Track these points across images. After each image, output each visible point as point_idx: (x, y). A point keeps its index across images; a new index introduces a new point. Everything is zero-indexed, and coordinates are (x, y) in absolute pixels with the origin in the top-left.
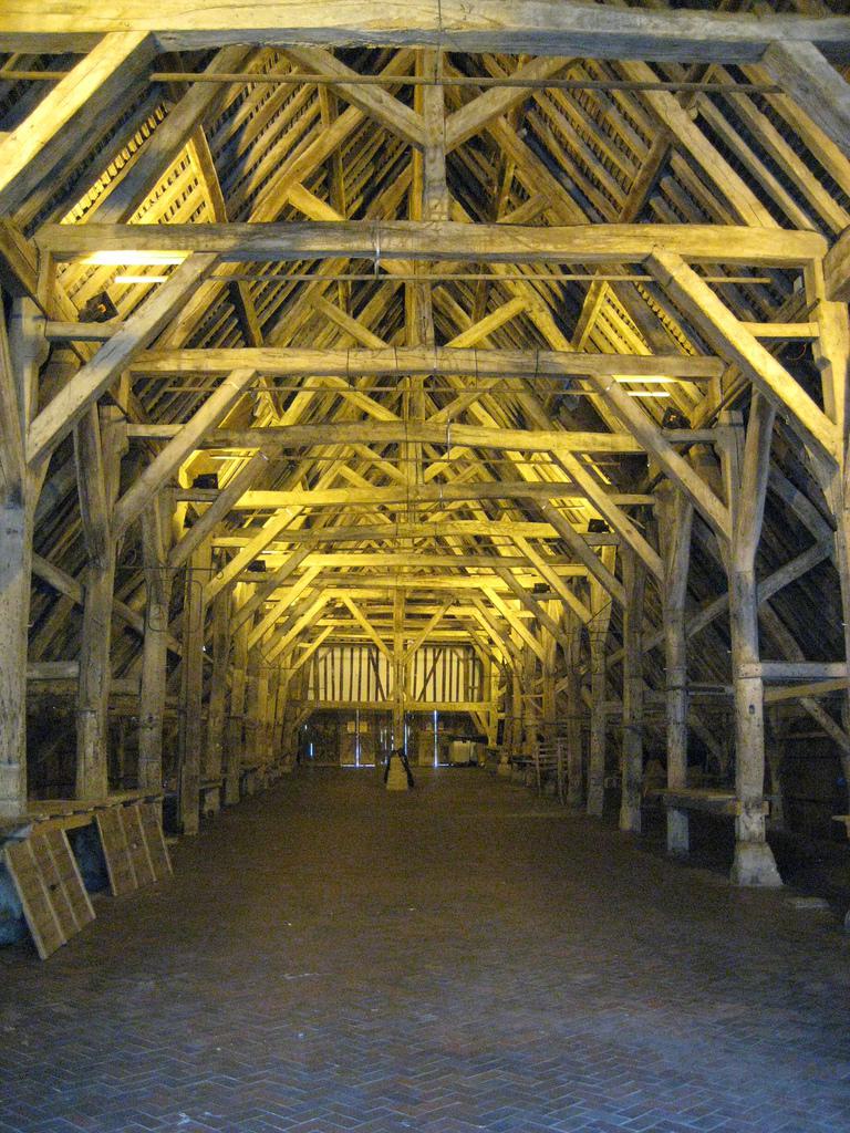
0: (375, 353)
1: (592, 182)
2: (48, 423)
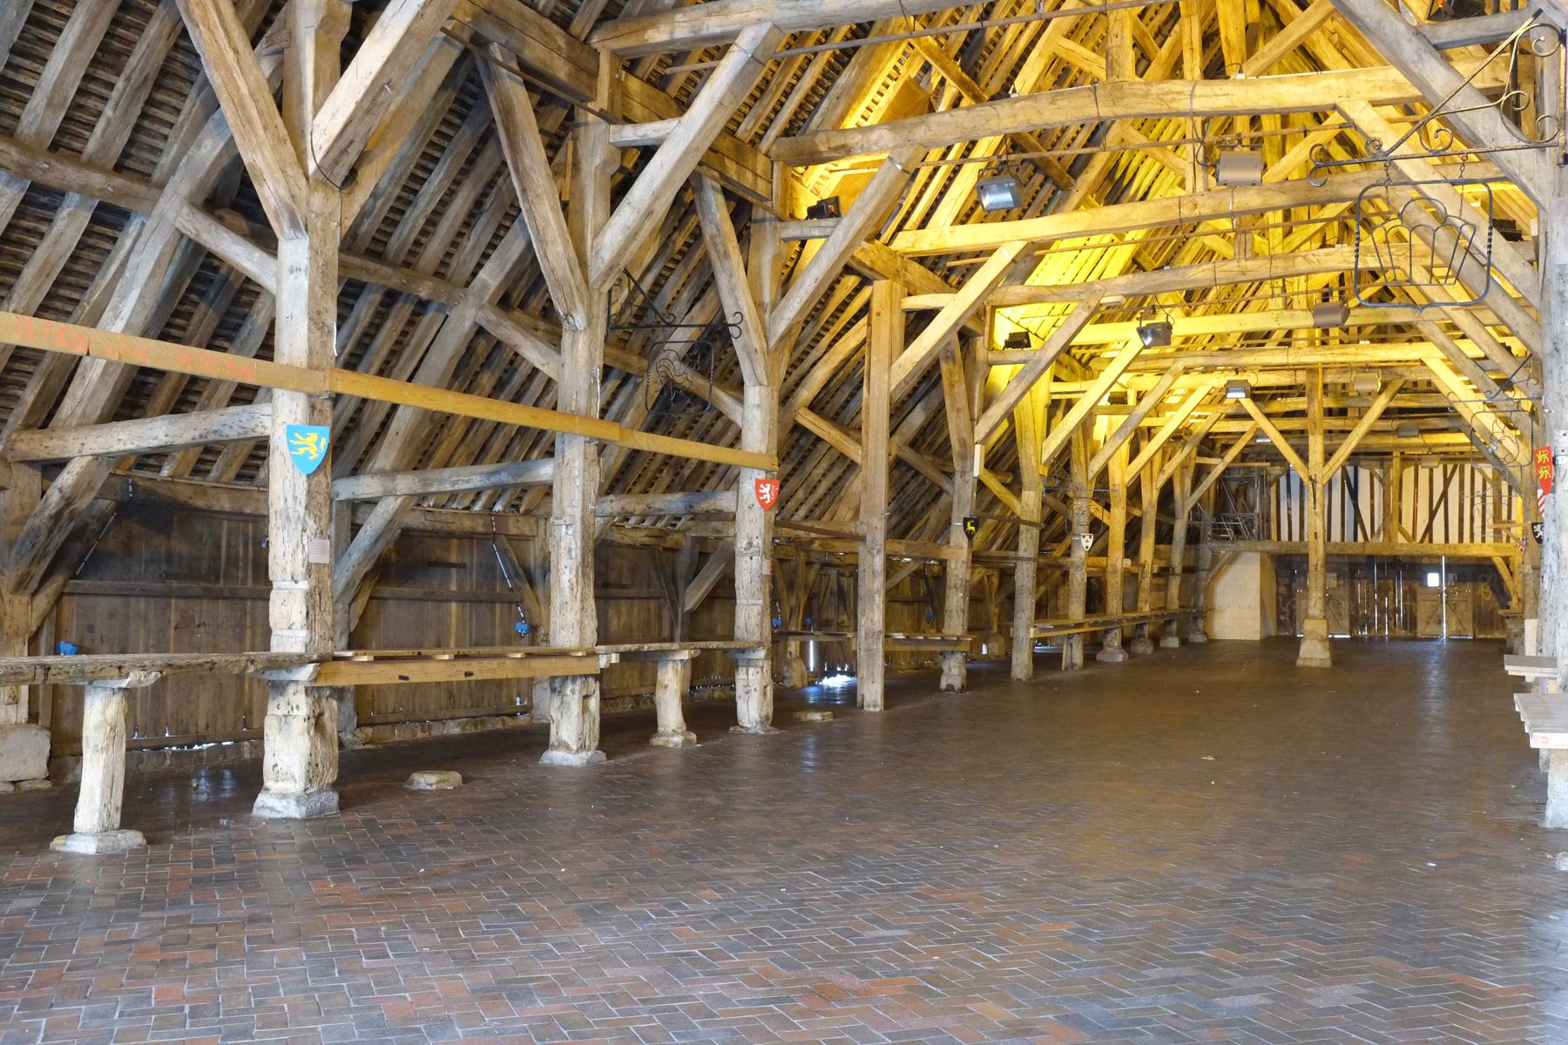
2: (333, 115)
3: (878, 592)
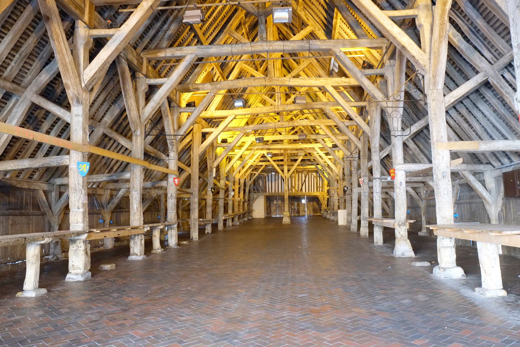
0: (243, 45)
2: (91, 71)
3: (197, 208)
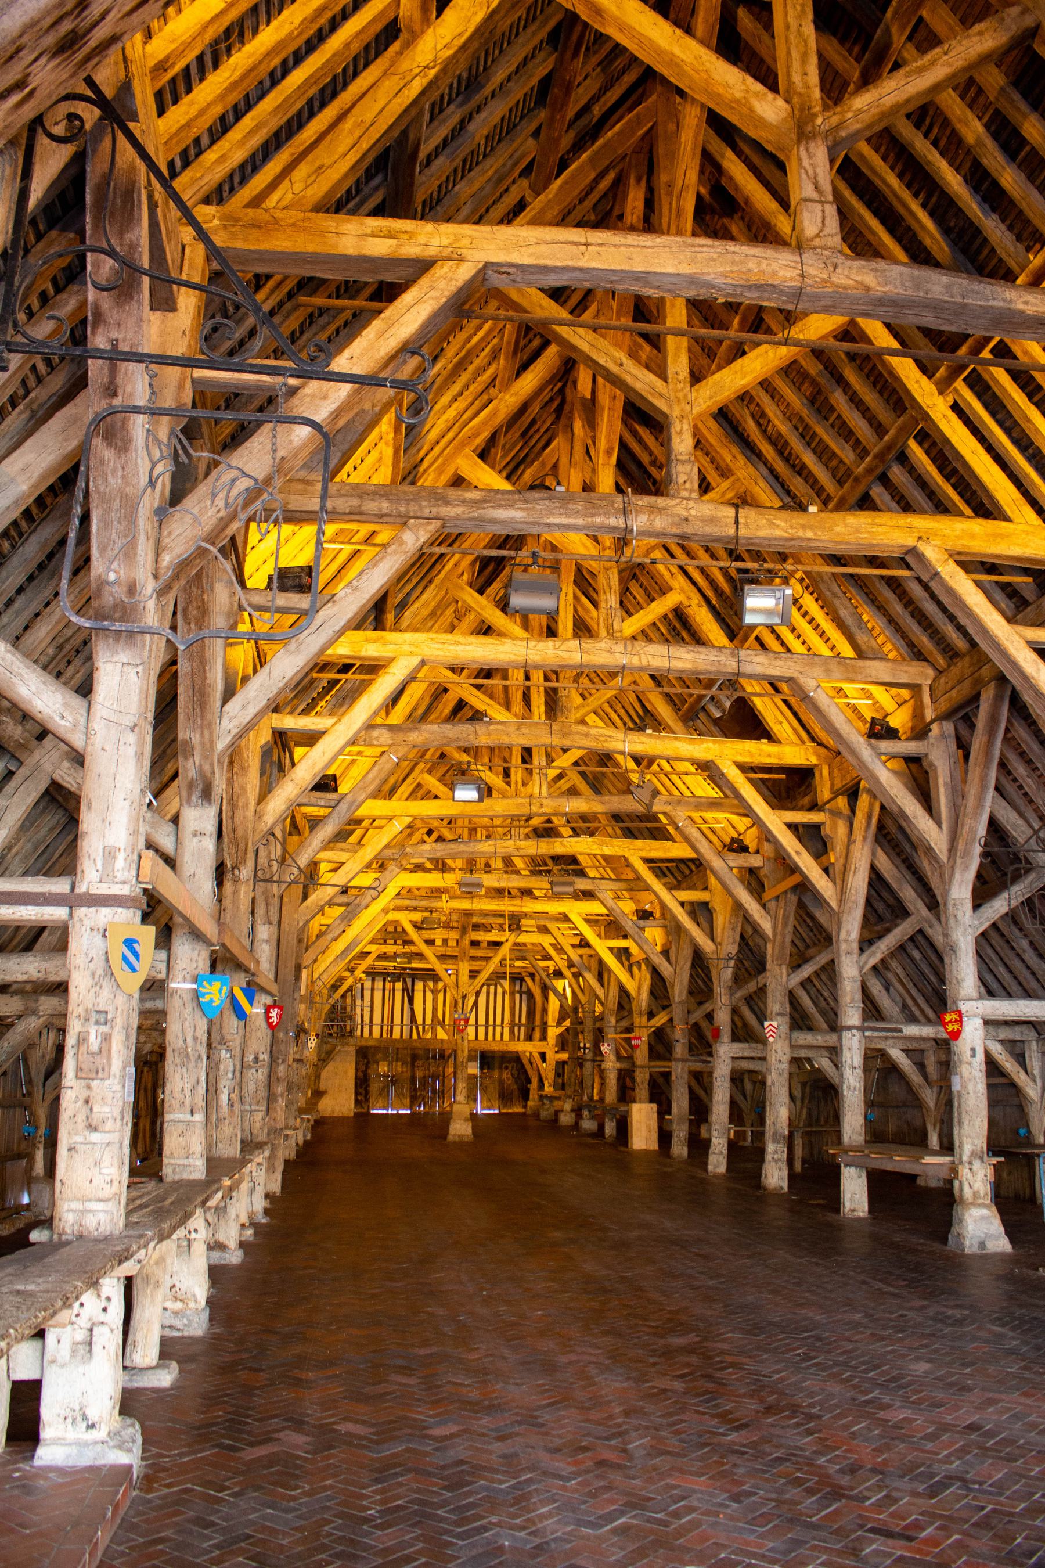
1: (793, 467)
3: (282, 1095)
